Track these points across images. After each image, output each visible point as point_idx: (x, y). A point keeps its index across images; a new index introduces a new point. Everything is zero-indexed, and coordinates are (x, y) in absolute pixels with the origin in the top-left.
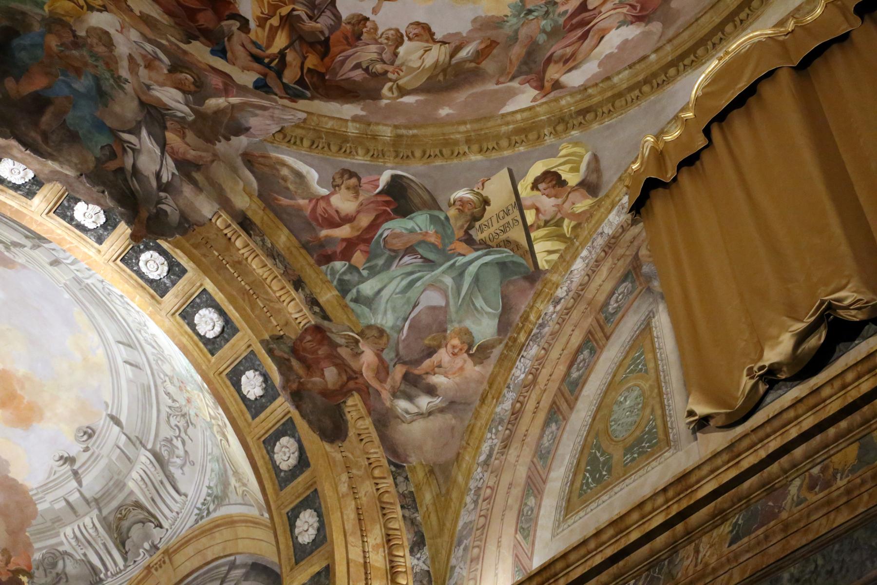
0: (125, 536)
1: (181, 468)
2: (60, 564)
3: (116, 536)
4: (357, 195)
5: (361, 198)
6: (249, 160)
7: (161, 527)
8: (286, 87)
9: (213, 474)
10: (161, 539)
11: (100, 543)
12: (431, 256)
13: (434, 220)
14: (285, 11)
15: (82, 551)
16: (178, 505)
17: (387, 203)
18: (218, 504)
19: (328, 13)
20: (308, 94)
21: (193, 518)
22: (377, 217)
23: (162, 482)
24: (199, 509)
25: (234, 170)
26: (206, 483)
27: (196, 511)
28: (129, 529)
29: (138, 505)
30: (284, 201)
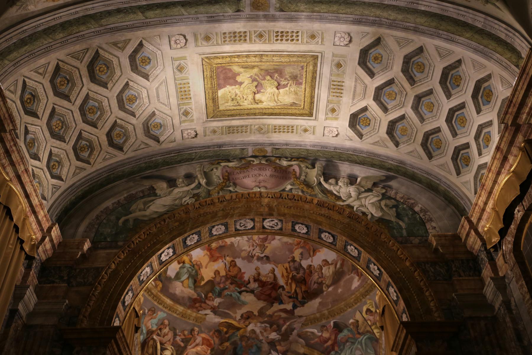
4: (328, 331)
5: (329, 331)
6: (299, 336)
8: (300, 302)
12: (353, 341)
13: (349, 331)
14: (291, 276)
17: (336, 330)
19: (301, 269)
20: (306, 301)
22: (335, 335)
25: (297, 342)
30: (312, 342)
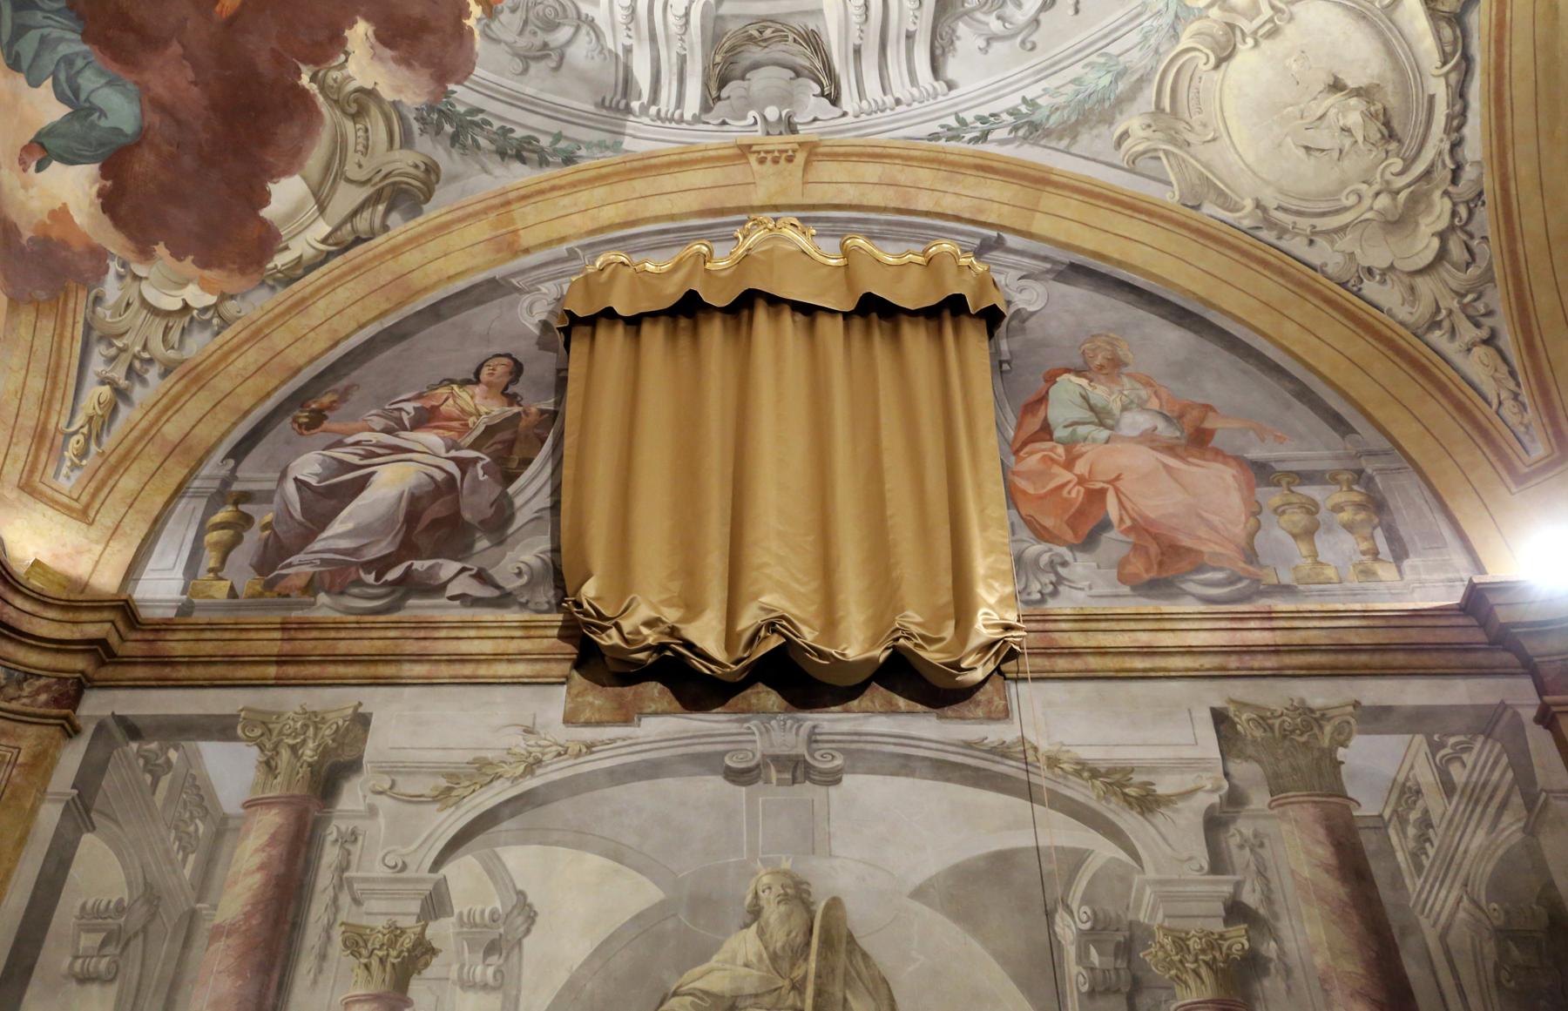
0: (737, 72)
1: (988, 44)
2: (564, 33)
3: (718, 59)
7: (835, 101)
9: (1071, 89)
10: (815, 120)
11: (676, 46)
15: (628, 42)
16: (915, 91)
18: (1025, 138)
21: (934, 127)
23: (910, 36)
24: (962, 122)
26: (1030, 93)
27: (952, 122)
28: (756, 66)
29: (813, 41)
